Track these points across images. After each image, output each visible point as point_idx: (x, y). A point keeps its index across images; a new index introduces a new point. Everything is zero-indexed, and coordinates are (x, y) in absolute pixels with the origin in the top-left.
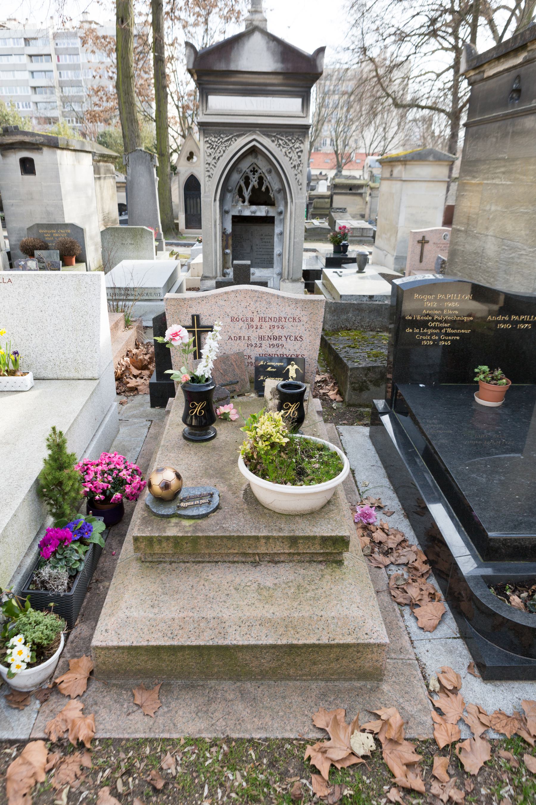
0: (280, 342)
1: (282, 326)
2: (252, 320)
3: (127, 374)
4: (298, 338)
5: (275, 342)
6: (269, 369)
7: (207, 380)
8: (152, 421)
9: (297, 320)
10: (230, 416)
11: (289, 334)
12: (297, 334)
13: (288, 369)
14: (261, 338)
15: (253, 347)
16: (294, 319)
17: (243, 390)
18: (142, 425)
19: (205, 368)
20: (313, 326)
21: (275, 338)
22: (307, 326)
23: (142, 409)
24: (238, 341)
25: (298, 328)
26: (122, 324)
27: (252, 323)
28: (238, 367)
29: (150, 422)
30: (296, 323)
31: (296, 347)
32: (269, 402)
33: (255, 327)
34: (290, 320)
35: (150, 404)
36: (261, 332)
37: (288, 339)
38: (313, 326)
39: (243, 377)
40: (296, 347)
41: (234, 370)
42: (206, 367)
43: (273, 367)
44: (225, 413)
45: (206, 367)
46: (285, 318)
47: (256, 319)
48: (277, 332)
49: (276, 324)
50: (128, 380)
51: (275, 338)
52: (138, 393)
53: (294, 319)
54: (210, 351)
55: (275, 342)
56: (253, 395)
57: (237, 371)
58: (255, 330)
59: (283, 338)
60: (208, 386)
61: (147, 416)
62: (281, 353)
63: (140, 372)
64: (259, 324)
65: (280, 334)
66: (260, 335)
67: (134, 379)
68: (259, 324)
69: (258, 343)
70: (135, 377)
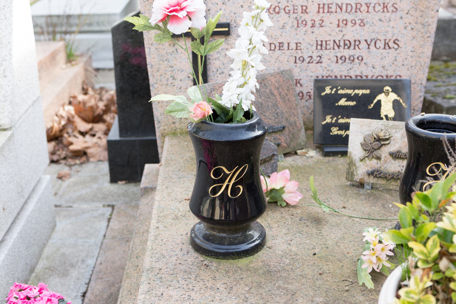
0: (357, 53)
1: (362, 21)
2: (305, 11)
3: (70, 130)
4: (391, 44)
5: (347, 53)
6: (342, 102)
7: (248, 115)
8: (113, 207)
9: (391, 9)
10: (285, 196)
11: (374, 36)
12: (389, 36)
13: (379, 102)
14: (321, 45)
15: (305, 64)
16: (385, 7)
17: (293, 144)
18: (95, 214)
19: (240, 90)
20: (420, 20)
21: (348, 45)
22: (409, 19)
23: (95, 186)
24: (278, 52)
25: (392, 24)
26: (62, 57)
27: (305, 16)
28: (283, 98)
29: (110, 209)
30: (388, 15)
31: (386, 62)
32: (358, 164)
33: (310, 24)
34: (378, 8)
35: (108, 178)
36: (321, 34)
37: (372, 47)
38: (420, 20)
39: (292, 119)
40: (386, 62)
41: (275, 105)
42: (241, 86)
43: (349, 98)
44: (273, 190)
45: (241, 86)
46: (368, 6)
47: (313, 9)
48: (351, 33)
49: (350, 17)
50: (71, 139)
51: (348, 45)
52: (88, 160)
53: (385, 7)
54: (250, 51)
55: (347, 53)
56: (312, 153)
57: (282, 107)
58: (310, 30)
59: (363, 45)
60: (251, 128)
61: (104, 198)
62: (358, 73)
63: (89, 126)
64: (317, 19)
65: (357, 37)
66: (319, 39)
67: (81, 137)
68: (317, 19)
69: (315, 55)
70: (83, 134)
